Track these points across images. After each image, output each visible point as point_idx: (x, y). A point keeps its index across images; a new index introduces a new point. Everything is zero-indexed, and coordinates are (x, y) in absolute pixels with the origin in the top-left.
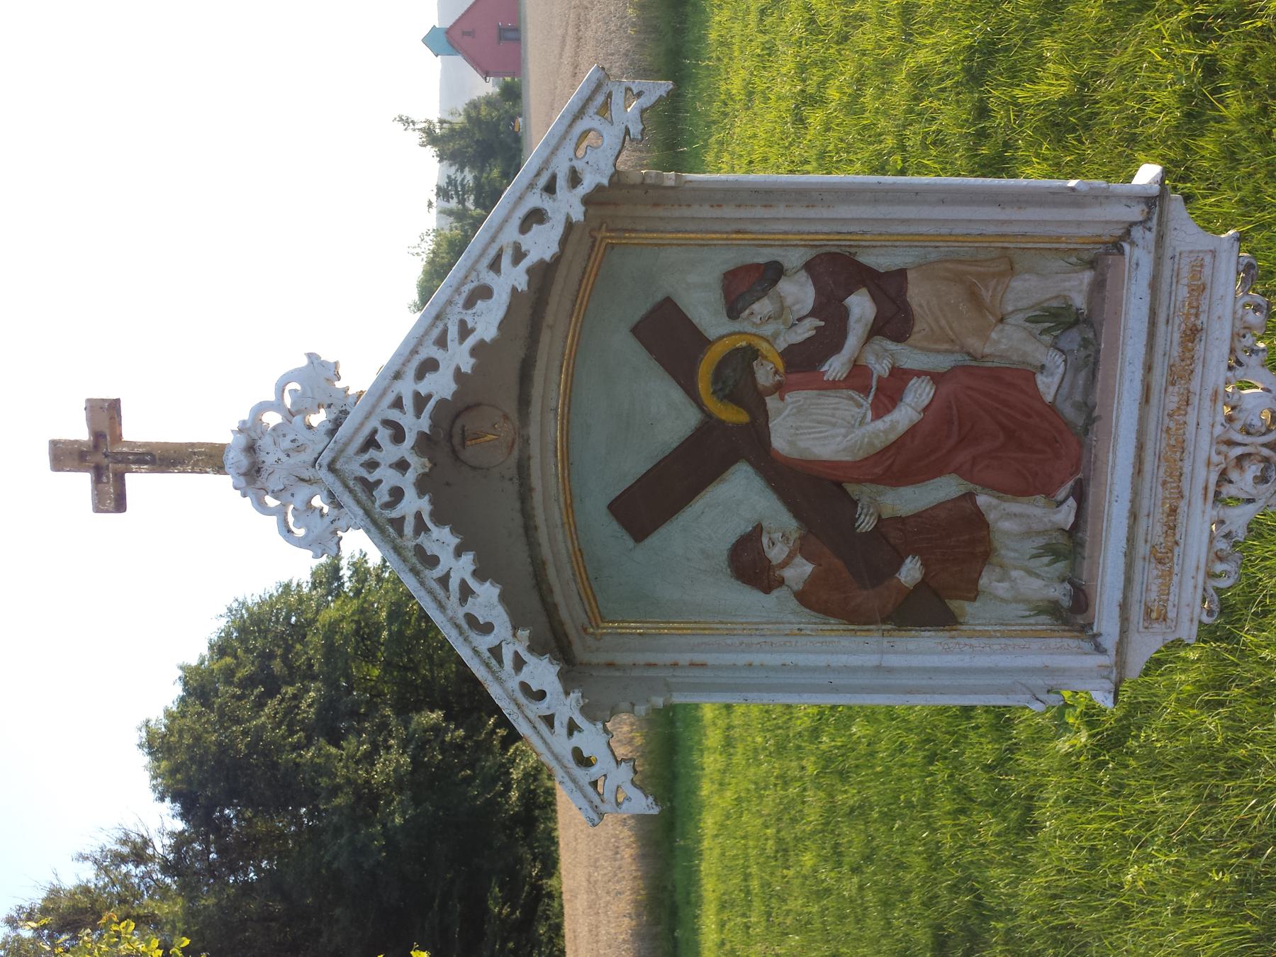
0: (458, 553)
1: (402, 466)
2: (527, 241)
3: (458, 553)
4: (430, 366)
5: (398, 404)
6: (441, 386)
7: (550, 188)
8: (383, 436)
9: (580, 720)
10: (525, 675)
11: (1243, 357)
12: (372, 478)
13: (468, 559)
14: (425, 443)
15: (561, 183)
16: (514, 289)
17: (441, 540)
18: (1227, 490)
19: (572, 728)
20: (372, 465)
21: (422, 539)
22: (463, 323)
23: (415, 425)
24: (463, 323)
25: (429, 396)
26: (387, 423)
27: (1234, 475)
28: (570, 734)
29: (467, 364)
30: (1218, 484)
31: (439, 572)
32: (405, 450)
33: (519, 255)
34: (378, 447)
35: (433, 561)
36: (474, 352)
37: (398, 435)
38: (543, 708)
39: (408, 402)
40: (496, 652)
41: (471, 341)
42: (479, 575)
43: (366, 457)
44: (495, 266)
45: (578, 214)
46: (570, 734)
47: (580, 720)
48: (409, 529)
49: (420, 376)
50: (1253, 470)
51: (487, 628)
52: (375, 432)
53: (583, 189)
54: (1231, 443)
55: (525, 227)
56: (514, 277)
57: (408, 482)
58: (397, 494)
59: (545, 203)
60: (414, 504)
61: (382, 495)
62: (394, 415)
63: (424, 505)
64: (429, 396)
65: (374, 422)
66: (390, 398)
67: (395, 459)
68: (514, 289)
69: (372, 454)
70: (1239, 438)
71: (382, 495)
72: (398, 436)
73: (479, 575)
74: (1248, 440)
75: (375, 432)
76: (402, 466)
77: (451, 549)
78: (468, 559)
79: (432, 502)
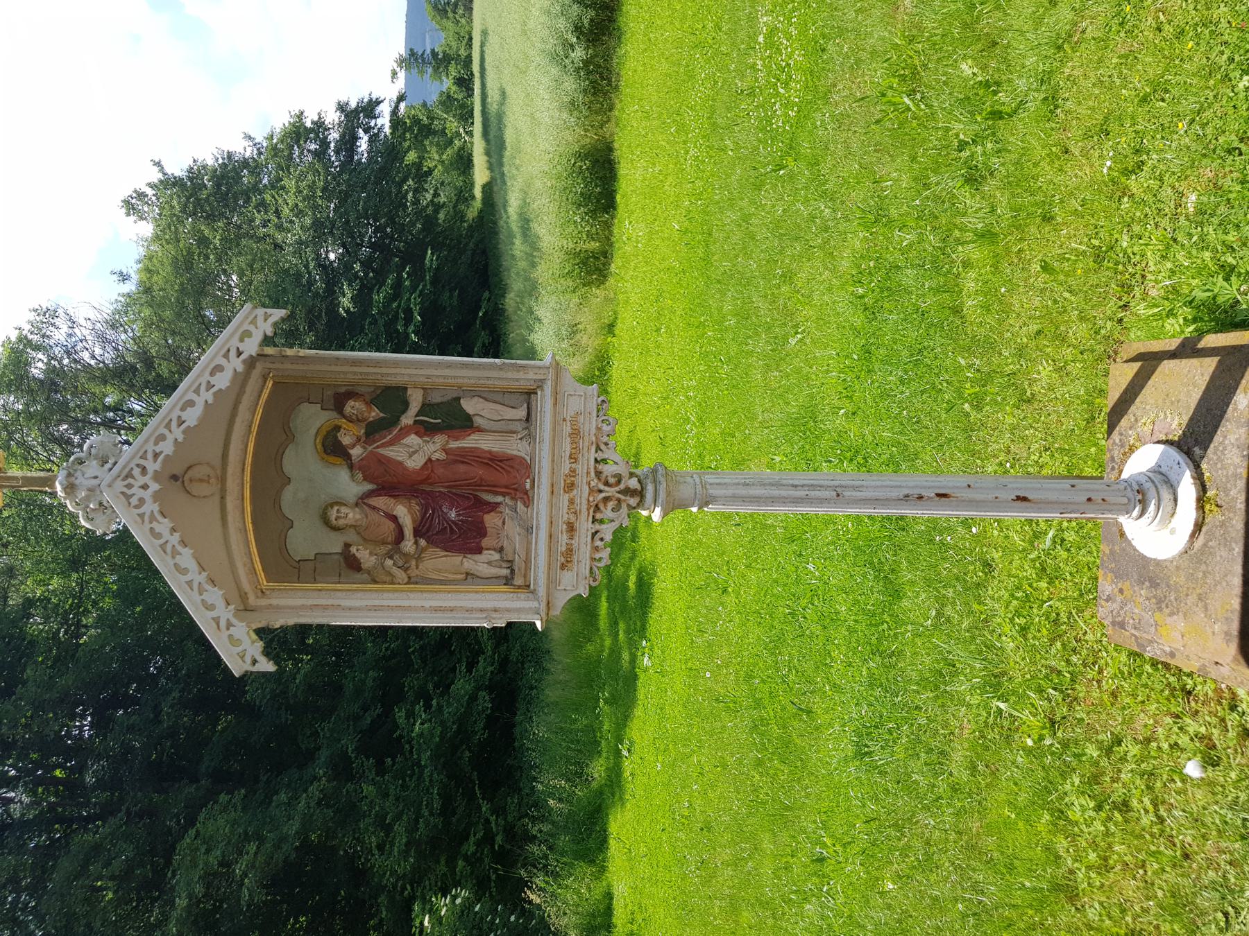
0: (173, 530)
1: (145, 487)
2: (213, 381)
3: (173, 530)
4: (162, 438)
5: (144, 457)
6: (167, 448)
7: (226, 356)
8: (137, 472)
9: (234, 621)
10: (205, 596)
11: (603, 447)
12: (129, 492)
13: (177, 536)
14: (157, 477)
15: (233, 353)
16: (206, 401)
17: (163, 526)
18: (598, 516)
19: (229, 625)
20: (129, 486)
21: (155, 525)
22: (179, 417)
23: (152, 467)
24: (179, 417)
25: (162, 452)
26: (138, 465)
27: (601, 506)
28: (228, 629)
29: (180, 438)
30: (594, 512)
31: (162, 541)
32: (147, 479)
33: (210, 386)
34: (133, 477)
35: (157, 536)
36: (184, 432)
37: (144, 470)
38: (214, 614)
39: (150, 456)
40: (190, 583)
41: (184, 426)
42: (183, 543)
43: (125, 483)
44: (197, 391)
45: (240, 368)
46: (228, 629)
47: (234, 621)
48: (146, 518)
49: (156, 443)
50: (611, 505)
51: (184, 571)
52: (132, 469)
53: (243, 357)
54: (600, 491)
55: (212, 374)
56: (209, 396)
57: (147, 495)
58: (142, 501)
59: (223, 362)
60: (151, 507)
61: (134, 501)
62: (142, 462)
63: (156, 507)
64: (162, 452)
65: (132, 465)
66: (141, 454)
67: (140, 484)
68: (206, 401)
69: (130, 480)
70: (602, 487)
71: (134, 501)
72: (144, 470)
73: (183, 543)
74: (606, 488)
75: (132, 469)
76: (145, 487)
77: (168, 530)
78: (177, 536)
79: (160, 505)
